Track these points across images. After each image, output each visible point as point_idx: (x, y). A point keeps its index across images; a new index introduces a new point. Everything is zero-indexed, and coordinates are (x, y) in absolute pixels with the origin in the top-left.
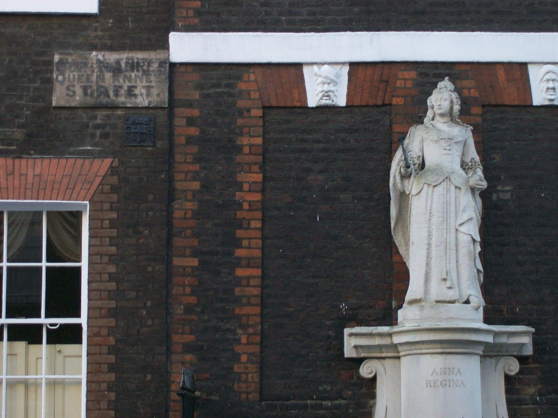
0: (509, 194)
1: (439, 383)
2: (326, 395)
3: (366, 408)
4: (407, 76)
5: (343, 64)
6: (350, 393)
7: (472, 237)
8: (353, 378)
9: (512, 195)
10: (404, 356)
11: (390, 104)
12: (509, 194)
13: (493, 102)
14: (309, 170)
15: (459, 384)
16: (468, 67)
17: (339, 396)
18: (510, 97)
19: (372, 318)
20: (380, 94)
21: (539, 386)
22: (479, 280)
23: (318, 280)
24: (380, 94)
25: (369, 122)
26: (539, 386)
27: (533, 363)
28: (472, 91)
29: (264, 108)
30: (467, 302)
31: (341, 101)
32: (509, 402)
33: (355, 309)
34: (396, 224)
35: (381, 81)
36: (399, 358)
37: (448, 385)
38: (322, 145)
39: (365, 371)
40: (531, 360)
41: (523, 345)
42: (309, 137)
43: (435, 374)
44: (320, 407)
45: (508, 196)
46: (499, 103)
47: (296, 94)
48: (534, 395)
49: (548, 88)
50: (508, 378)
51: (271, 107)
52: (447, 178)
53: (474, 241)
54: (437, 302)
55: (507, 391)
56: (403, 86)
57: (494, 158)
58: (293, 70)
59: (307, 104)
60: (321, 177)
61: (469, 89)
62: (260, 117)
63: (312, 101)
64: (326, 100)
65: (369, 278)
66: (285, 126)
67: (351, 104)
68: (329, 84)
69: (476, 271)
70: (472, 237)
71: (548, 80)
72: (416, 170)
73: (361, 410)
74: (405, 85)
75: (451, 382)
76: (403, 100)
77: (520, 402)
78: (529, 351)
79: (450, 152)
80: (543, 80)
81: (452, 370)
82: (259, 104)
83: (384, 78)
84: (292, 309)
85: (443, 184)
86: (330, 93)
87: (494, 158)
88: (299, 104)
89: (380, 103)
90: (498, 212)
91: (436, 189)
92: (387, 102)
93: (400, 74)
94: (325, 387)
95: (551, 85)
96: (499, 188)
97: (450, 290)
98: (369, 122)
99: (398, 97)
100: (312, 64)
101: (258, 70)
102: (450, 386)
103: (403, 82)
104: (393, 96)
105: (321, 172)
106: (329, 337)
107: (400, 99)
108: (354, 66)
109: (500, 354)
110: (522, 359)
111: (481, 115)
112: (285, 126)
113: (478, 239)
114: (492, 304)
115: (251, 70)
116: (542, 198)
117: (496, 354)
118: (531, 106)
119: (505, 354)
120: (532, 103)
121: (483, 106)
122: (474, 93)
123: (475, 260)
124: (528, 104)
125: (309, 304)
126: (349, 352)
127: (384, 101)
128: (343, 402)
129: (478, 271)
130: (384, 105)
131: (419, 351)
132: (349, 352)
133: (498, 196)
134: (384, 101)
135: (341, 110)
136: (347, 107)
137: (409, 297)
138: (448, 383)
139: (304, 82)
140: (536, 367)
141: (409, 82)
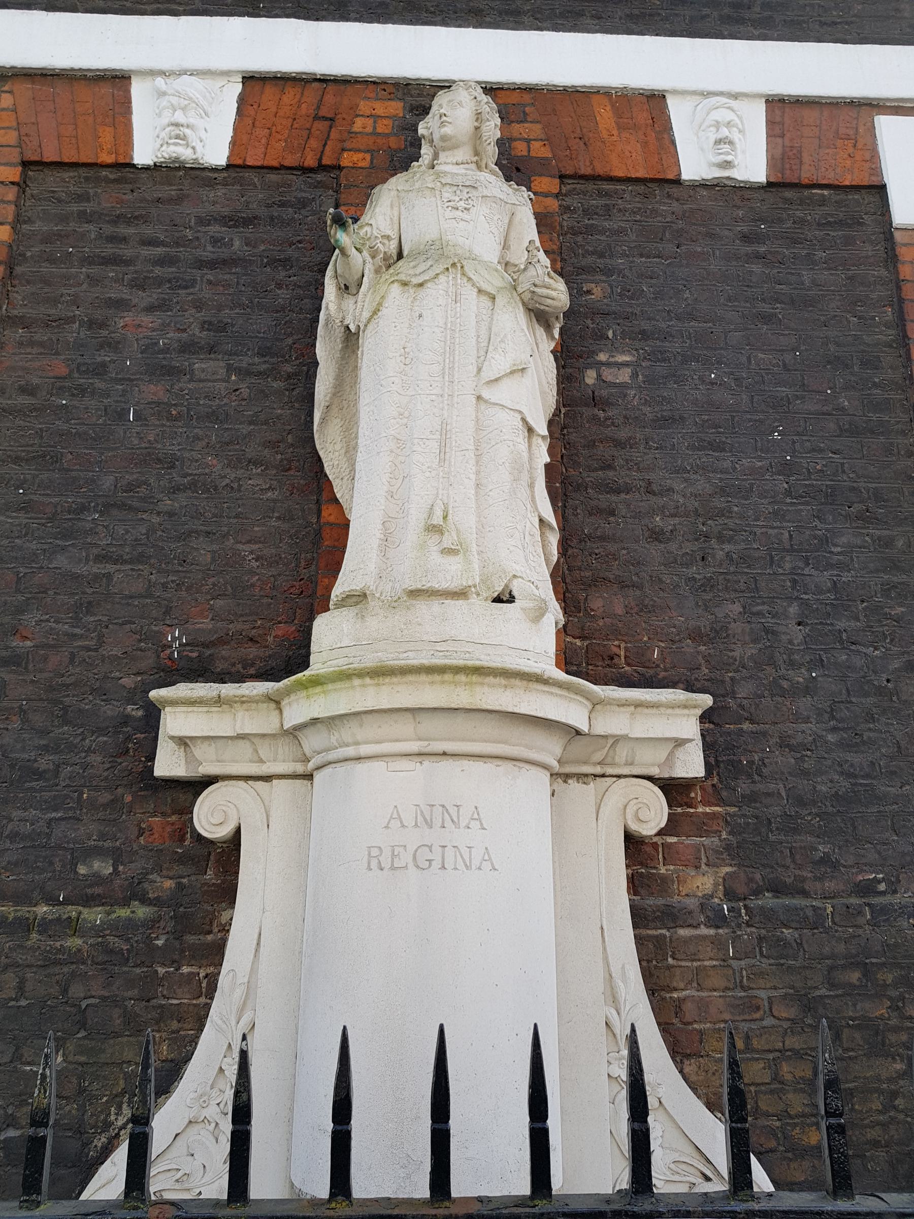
0: (628, 371)
1: (406, 858)
2: (98, 890)
3: (210, 932)
4: (380, 111)
5: (227, 73)
6: (169, 884)
7: (524, 420)
8: (182, 839)
9: (634, 375)
10: (318, 768)
11: (339, 168)
12: (628, 371)
13: (585, 170)
14: (120, 305)
15: (476, 863)
16: (527, 98)
17: (135, 893)
18: (627, 158)
19: (252, 671)
20: (314, 143)
21: (728, 869)
22: (547, 560)
23: (110, 568)
24: (314, 143)
25: (282, 204)
26: (728, 869)
27: (705, 803)
28: (536, 145)
29: (26, 164)
30: (504, 598)
31: (214, 150)
32: (639, 917)
33: (205, 645)
34: (323, 420)
35: (316, 118)
36: (309, 777)
37: (436, 865)
38: (160, 250)
39: (210, 817)
40: (696, 794)
41: (679, 743)
42: (131, 231)
43: (395, 824)
44: (73, 926)
45: (624, 376)
46: (600, 170)
47: (107, 136)
48: (712, 896)
49: (718, 142)
50: (632, 841)
51: (41, 164)
52: (454, 265)
53: (530, 430)
54: (414, 594)
55: (635, 884)
56: (369, 129)
57: (589, 292)
58: (106, 90)
59: (132, 158)
60: (146, 320)
61: (528, 141)
62: (13, 183)
63: (143, 154)
64: (175, 144)
65: (255, 564)
66: (75, 208)
67: (240, 162)
68: (184, 109)
69: (537, 520)
70: (524, 420)
71: (717, 125)
72: (377, 271)
73: (191, 939)
74: (375, 128)
75: (450, 852)
76: (368, 157)
77: (672, 916)
78: (691, 764)
79: (465, 216)
80: (706, 123)
81: (453, 811)
82: (15, 156)
83: (324, 112)
84: (28, 643)
85: (442, 278)
86: (188, 132)
87: (589, 292)
88: (110, 159)
89: (310, 161)
90: (601, 414)
91: (422, 292)
92: (326, 161)
93: (364, 107)
94: (96, 865)
95: (724, 132)
96: (602, 357)
97: (452, 559)
98: (282, 204)
99: (359, 151)
100: (152, 73)
101: (24, 88)
102: (443, 867)
103: (370, 121)
104: (343, 150)
105: (150, 309)
106: (126, 720)
107: (361, 155)
108: (253, 82)
109: (610, 771)
110: (674, 789)
111: (557, 196)
112: (75, 208)
113: (542, 429)
114: (582, 638)
115: (6, 88)
116: (712, 383)
117: (598, 770)
118: (677, 182)
119: (626, 771)
120: (680, 174)
121: (562, 177)
122: (539, 150)
123: (531, 486)
124: (671, 176)
125: (77, 631)
126: (168, 764)
127: (320, 159)
128: (142, 912)
129: (541, 521)
130: (322, 168)
131: (350, 751)
132: (168, 764)
133: (599, 376)
134: (320, 159)
135: (216, 175)
136: (229, 166)
137: (338, 591)
138: (436, 856)
139: (131, 113)
140: (714, 815)
141: (385, 122)
